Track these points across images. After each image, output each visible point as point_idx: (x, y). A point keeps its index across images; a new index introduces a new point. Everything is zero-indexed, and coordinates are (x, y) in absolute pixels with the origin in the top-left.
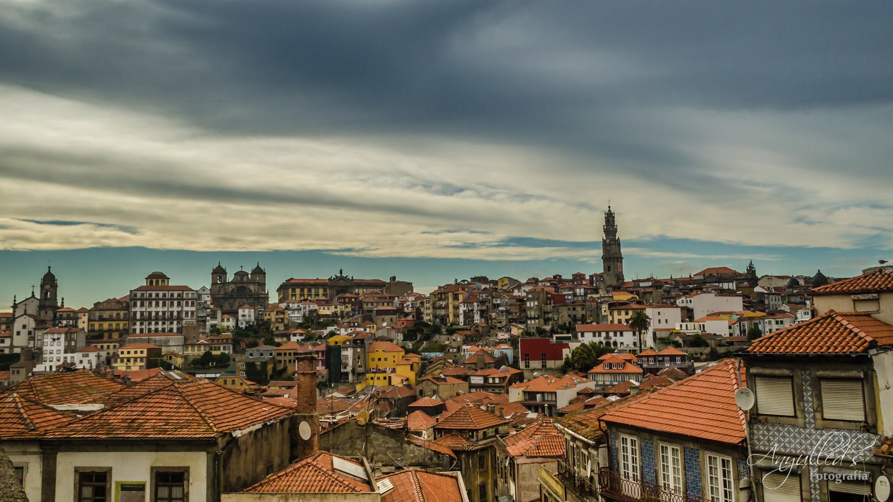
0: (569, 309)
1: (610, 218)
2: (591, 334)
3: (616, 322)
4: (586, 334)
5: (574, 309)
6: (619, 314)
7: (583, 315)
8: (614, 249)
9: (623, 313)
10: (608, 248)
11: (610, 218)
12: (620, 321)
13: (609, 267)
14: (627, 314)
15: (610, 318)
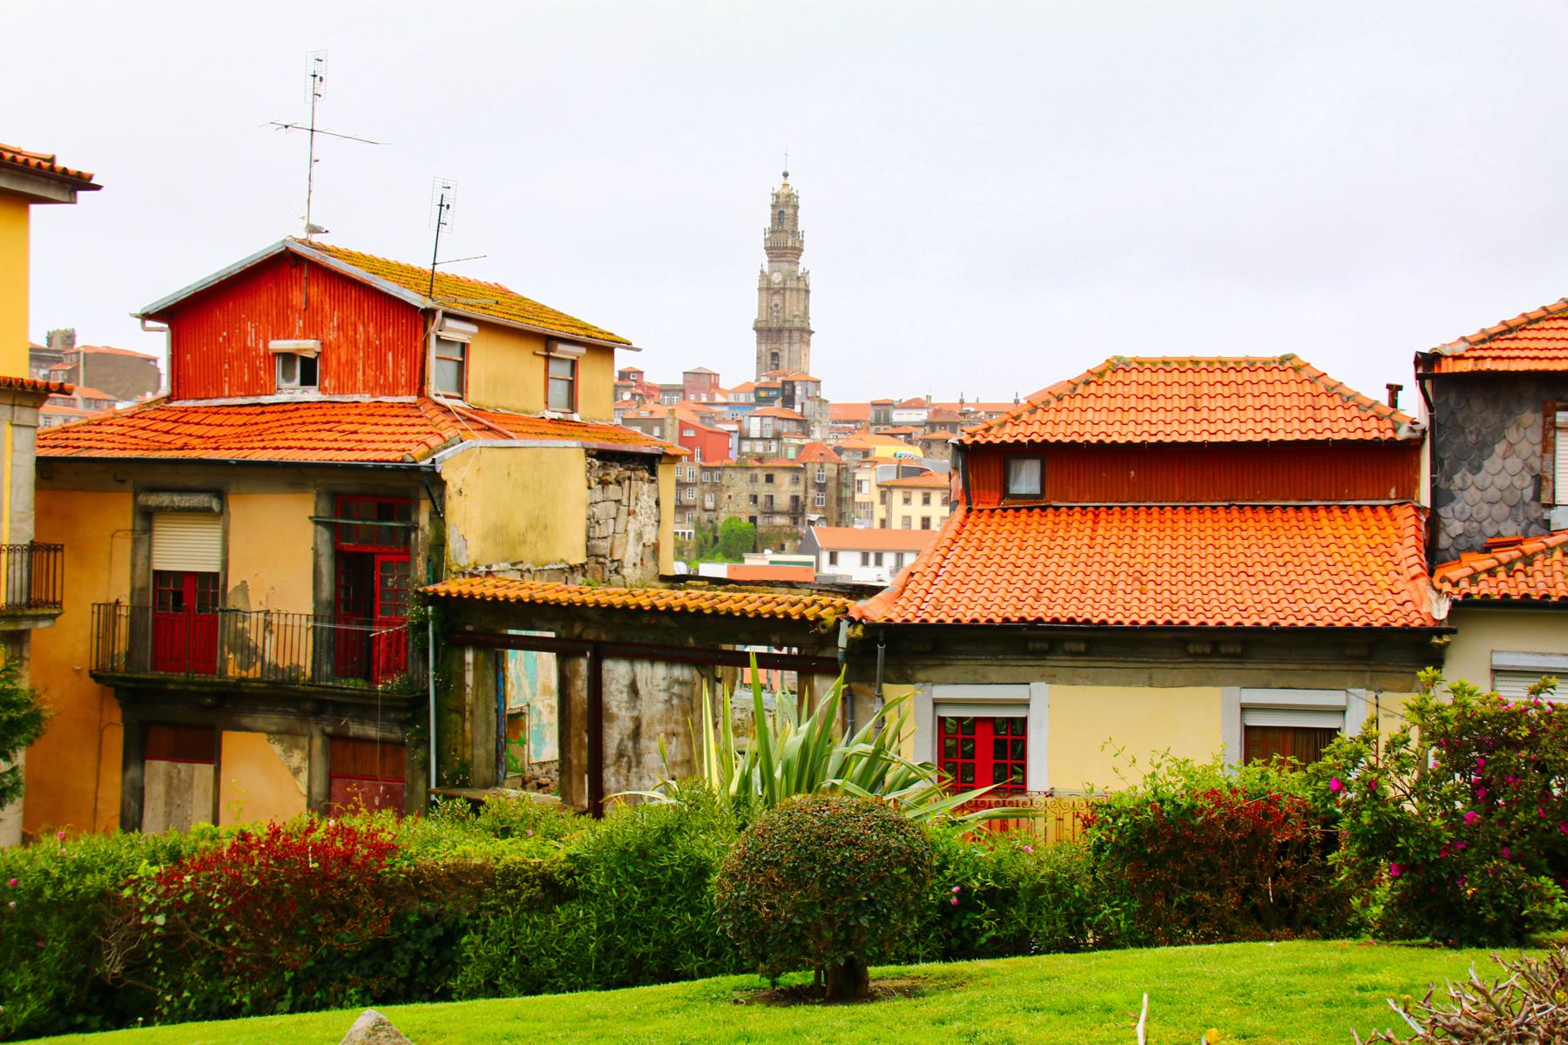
0: (754, 479)
1: (784, 212)
2: (857, 557)
3: (896, 524)
4: (841, 556)
5: (770, 479)
6: (907, 501)
7: (795, 499)
8: (792, 305)
9: (917, 497)
10: (777, 299)
11: (784, 212)
12: (907, 520)
13: (775, 355)
14: (926, 501)
15: (879, 512)
